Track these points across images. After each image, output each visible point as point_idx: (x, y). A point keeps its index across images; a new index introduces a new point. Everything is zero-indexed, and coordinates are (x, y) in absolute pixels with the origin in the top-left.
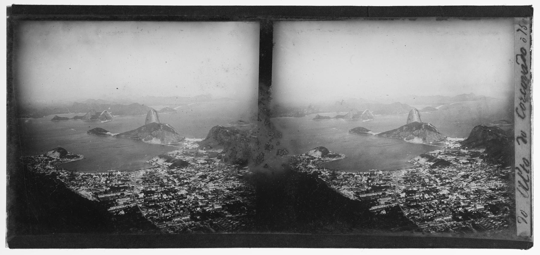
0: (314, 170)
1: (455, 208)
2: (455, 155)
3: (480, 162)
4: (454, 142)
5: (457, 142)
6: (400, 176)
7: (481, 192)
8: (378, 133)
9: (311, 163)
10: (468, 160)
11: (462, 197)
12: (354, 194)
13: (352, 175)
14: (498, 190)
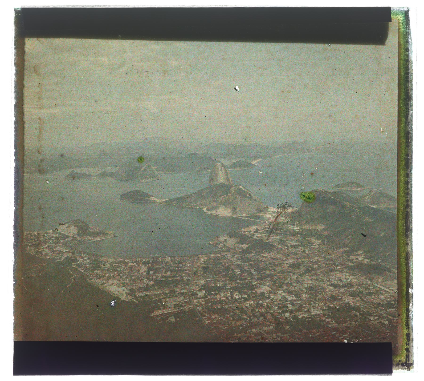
0: (66, 255)
1: (279, 313)
7: (318, 290)
10: (298, 240)
11: (290, 298)
12: (127, 291)
13: (125, 262)
14: (344, 286)
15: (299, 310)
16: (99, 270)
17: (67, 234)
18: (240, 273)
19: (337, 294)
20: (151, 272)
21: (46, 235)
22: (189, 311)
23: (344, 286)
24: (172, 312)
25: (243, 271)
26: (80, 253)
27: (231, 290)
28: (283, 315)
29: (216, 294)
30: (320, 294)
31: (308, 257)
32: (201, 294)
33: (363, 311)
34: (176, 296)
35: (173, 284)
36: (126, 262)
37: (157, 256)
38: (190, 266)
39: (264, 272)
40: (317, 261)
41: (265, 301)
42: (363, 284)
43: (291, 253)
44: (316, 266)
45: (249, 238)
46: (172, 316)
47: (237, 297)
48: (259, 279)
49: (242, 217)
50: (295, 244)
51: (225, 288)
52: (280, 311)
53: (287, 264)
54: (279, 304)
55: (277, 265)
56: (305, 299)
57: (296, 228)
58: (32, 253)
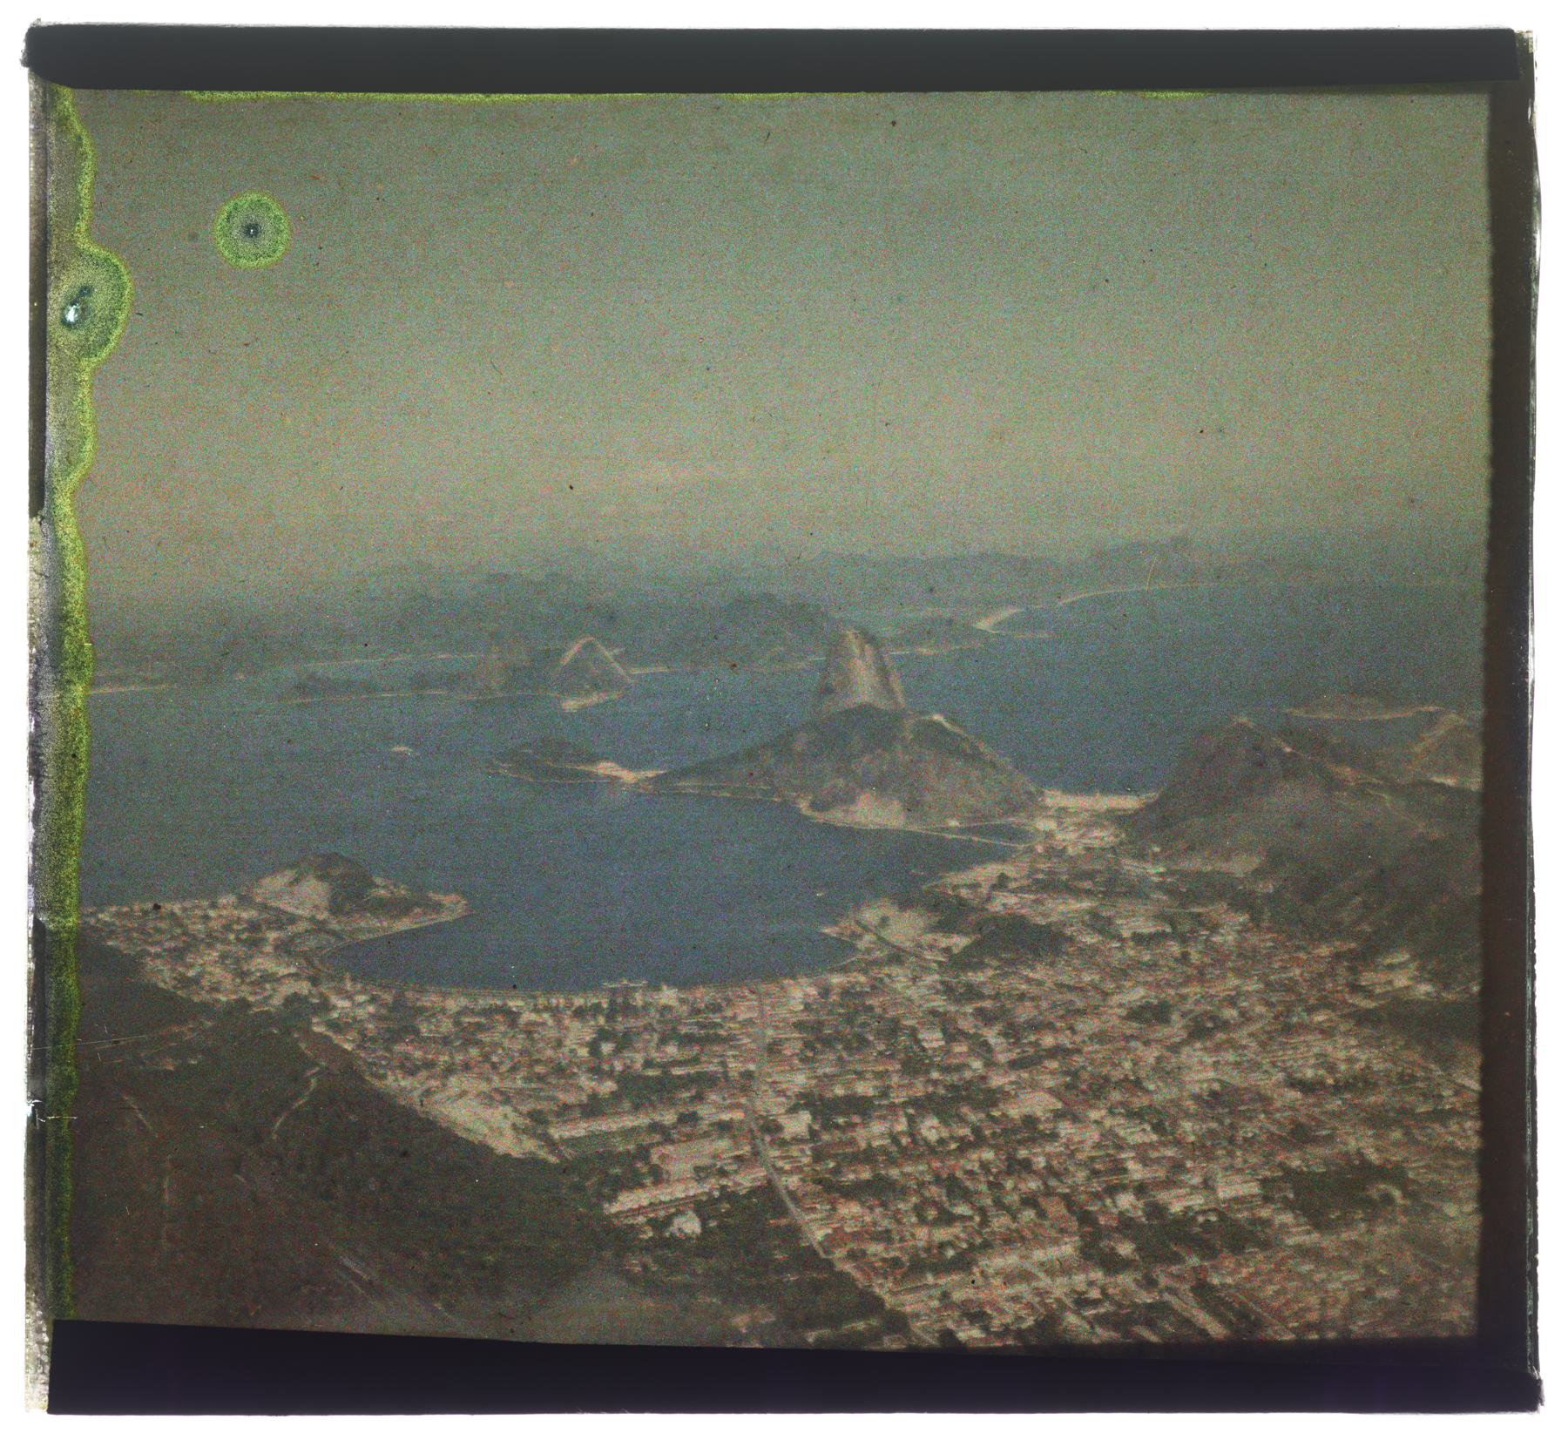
0: (287, 989)
1: (1097, 1196)
2: (1088, 893)
3: (1230, 929)
4: (1084, 816)
5: (1097, 820)
6: (783, 1012)
7: (1243, 1103)
8: (650, 774)
9: (268, 949)
10: (1161, 917)
12: (520, 1121)
14: (1337, 1089)
15: (1169, 1183)
16: (412, 1041)
17: (290, 909)
18: (943, 1043)
19: (1314, 1119)
20: (607, 1048)
21: (212, 913)
22: (753, 1192)
23: (1337, 1089)
24: (687, 1197)
25: (952, 1035)
26: (342, 979)
27: (911, 1111)
28: (1108, 1201)
29: (851, 1126)
30: (1250, 1119)
31: (1201, 977)
32: (798, 1124)
33: (1414, 1181)
34: (706, 1135)
35: (689, 1090)
36: (514, 1009)
37: (627, 987)
38: (750, 1022)
39: (1032, 1038)
40: (1233, 993)
41: (1039, 1150)
42: (1413, 1078)
43: (1137, 965)
44: (1230, 1013)
45: (973, 909)
46: (690, 1213)
47: (932, 1136)
48: (1014, 1065)
49: (949, 830)
50: (1147, 928)
51: (885, 1102)
52: (1096, 1186)
53: (1121, 1005)
54: (1092, 1159)
55: (1081, 1013)
56: (1192, 1138)
57: (1154, 870)
58: (165, 983)
